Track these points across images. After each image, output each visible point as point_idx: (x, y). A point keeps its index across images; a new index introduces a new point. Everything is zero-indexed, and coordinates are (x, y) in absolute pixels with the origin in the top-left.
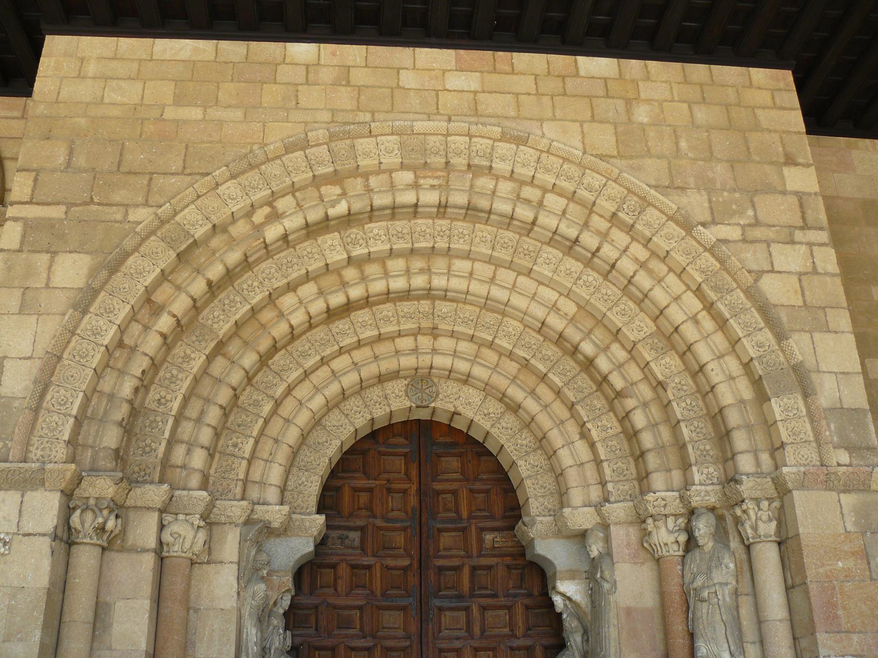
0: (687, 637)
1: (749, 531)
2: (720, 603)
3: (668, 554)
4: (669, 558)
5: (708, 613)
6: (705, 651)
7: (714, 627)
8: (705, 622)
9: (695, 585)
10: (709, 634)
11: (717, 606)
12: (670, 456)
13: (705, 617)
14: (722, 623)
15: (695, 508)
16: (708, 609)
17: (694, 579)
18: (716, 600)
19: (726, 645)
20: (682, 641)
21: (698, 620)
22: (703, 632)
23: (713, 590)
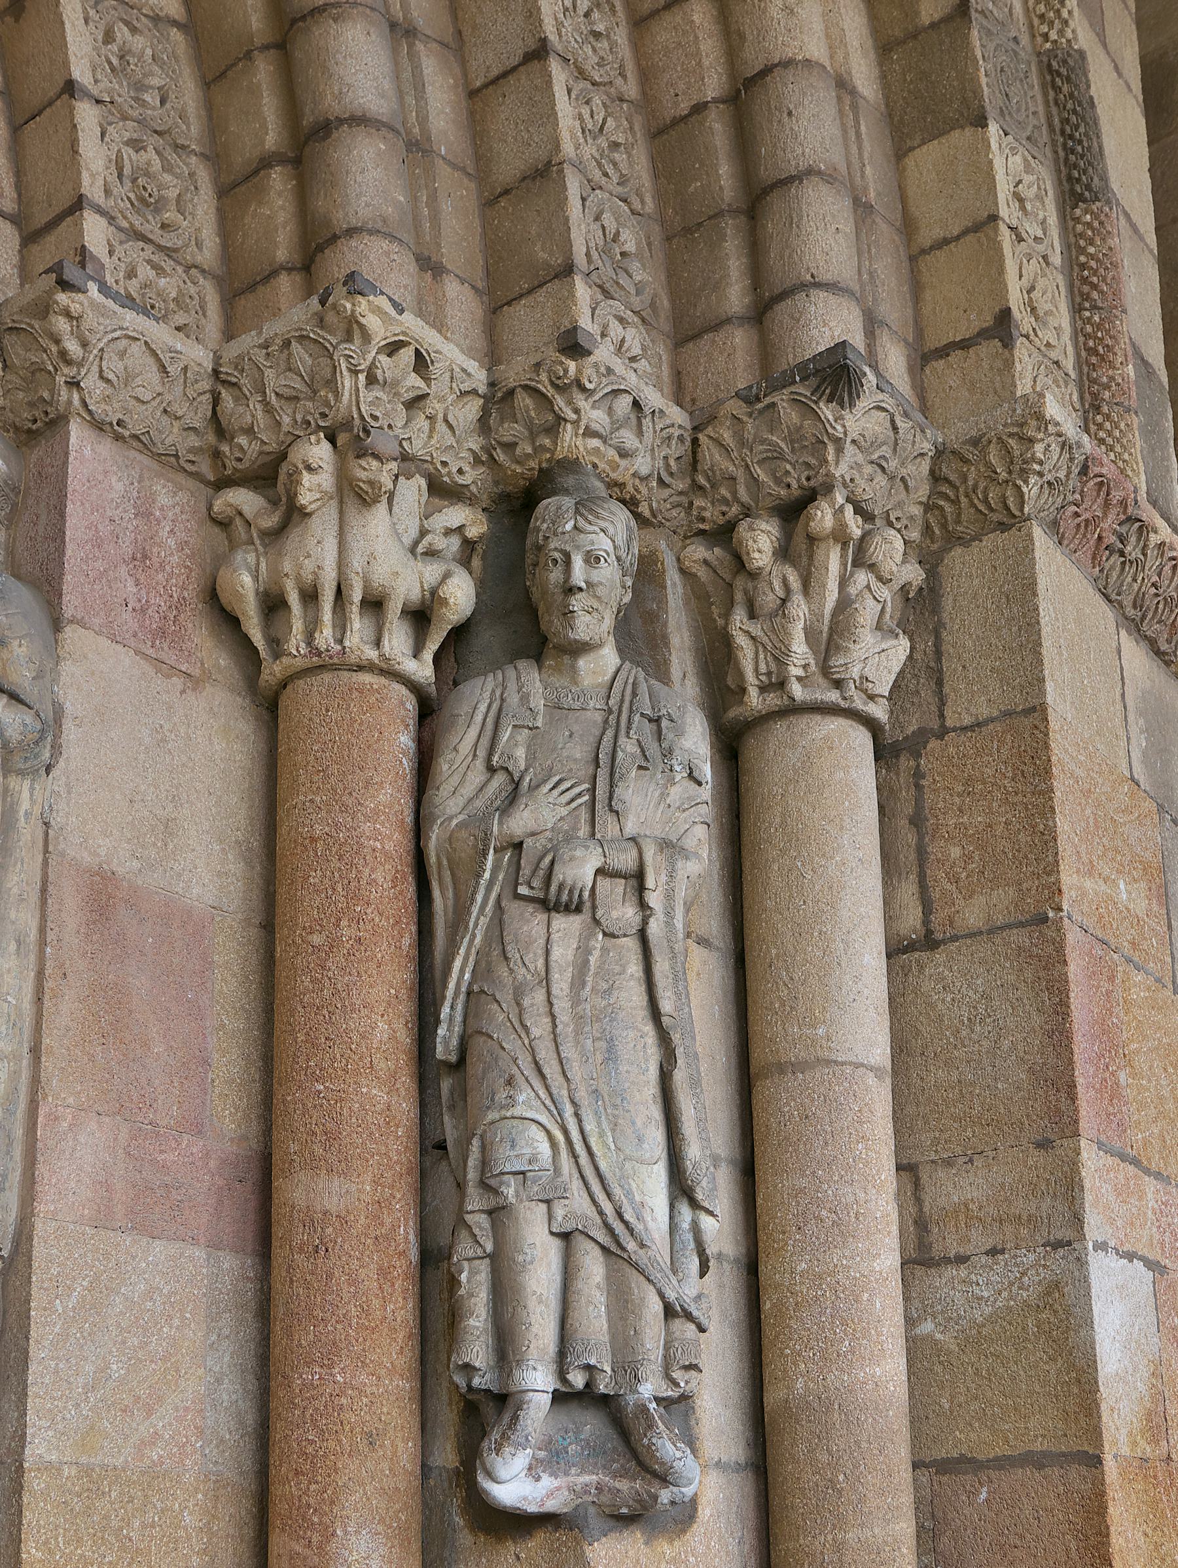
0: (406, 1082)
1: (799, 648)
2: (655, 928)
3: (372, 654)
4: (366, 678)
5: (582, 967)
6: (544, 1148)
7: (611, 1041)
8: (562, 1006)
9: (521, 822)
10: (576, 1071)
11: (631, 945)
12: (446, 206)
13: (561, 984)
14: (649, 1029)
15: (571, 465)
16: (584, 951)
17: (513, 796)
18: (629, 913)
19: (656, 1136)
20: (379, 1094)
21: (518, 993)
22: (545, 1053)
23: (625, 860)
